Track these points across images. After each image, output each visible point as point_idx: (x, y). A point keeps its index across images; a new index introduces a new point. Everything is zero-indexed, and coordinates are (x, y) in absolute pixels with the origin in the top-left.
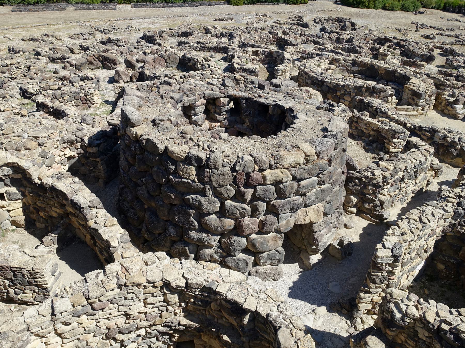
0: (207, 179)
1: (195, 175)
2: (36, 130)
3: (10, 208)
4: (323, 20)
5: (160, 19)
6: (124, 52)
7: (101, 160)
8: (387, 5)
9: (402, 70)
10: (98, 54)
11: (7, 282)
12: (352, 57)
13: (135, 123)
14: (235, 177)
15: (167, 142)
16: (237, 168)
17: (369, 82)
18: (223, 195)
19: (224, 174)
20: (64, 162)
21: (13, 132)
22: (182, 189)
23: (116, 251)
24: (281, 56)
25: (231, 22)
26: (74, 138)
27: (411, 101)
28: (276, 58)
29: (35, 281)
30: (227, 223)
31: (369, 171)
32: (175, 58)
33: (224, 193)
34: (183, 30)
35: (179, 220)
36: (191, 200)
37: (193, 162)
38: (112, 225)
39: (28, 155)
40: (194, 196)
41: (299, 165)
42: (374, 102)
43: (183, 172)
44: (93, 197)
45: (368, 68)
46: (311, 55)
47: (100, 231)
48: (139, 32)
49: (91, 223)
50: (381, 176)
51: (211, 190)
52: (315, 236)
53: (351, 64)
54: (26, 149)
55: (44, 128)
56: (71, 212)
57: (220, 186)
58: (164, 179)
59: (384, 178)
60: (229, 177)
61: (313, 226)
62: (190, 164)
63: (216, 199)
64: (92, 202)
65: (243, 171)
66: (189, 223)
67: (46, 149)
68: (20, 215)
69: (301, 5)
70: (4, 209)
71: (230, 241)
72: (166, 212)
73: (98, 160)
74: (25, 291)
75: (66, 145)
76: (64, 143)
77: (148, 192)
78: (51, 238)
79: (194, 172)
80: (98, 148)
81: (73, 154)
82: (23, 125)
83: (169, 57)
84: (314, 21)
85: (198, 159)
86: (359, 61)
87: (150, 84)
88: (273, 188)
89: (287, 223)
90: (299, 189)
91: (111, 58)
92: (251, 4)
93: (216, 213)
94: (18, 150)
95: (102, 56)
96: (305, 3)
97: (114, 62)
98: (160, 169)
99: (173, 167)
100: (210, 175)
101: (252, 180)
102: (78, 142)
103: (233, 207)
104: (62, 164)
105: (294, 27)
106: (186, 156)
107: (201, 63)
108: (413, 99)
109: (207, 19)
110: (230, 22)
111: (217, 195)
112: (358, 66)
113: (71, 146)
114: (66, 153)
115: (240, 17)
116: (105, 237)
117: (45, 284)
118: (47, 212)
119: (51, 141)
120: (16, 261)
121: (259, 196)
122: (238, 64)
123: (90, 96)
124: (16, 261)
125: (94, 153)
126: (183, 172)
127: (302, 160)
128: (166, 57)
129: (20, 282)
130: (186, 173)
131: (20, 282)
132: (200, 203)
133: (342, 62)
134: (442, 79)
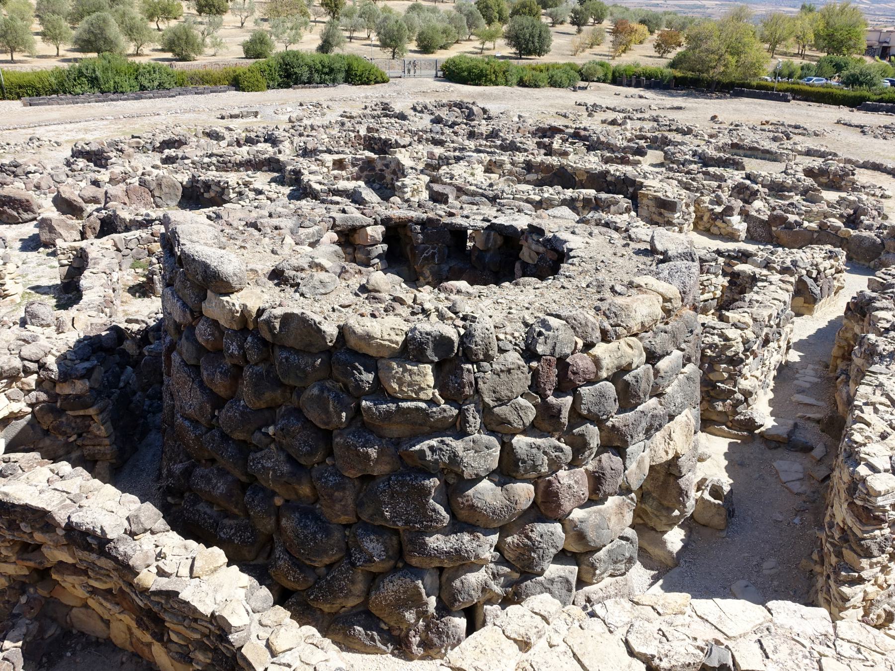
0: (468, 391)
4: (430, 107)
6: (44, 185)
7: (101, 411)
8: (526, 78)
9: (617, 170)
12: (520, 157)
13: (234, 282)
14: (535, 373)
15: (339, 317)
16: (540, 349)
17: (584, 191)
18: (509, 423)
19: (509, 371)
22: (395, 430)
23: (247, 638)
24: (393, 166)
25: (255, 119)
26: (17, 363)
27: (656, 218)
28: (382, 170)
30: (522, 494)
31: (713, 334)
32: (173, 186)
33: (513, 417)
34: (161, 138)
35: (396, 515)
36: (428, 453)
37: (430, 353)
38: (215, 570)
40: (434, 442)
42: (618, 221)
43: (400, 382)
44: (132, 502)
45: (555, 174)
46: (445, 161)
47: (184, 595)
49: (149, 579)
50: (740, 340)
51: (478, 417)
52: (683, 487)
53: (523, 168)
56: (61, 562)
57: (501, 402)
58: (344, 414)
59: (746, 342)
60: (521, 376)
61: (680, 464)
62: (420, 358)
63: (492, 438)
64: (137, 517)
66: (425, 515)
69: (377, 85)
71: (529, 538)
72: (350, 501)
73: (91, 411)
77: (291, 460)
79: (431, 380)
80: (89, 379)
81: (15, 407)
83: (160, 185)
84: (414, 109)
85: (443, 342)
86: (537, 162)
87: (144, 235)
88: (610, 388)
90: (659, 380)
91: (18, 197)
92: (282, 88)
93: (491, 475)
96: (384, 82)
97: (24, 206)
98: (329, 390)
99: (370, 377)
100: (476, 379)
101: (574, 373)
102: (27, 372)
103: (534, 451)
105: (385, 120)
106: (405, 342)
107: (237, 190)
108: (661, 214)
109: (204, 117)
110: (252, 119)
111: (494, 427)
112: (536, 172)
115: (270, 111)
116: (206, 608)
121: (589, 410)
122: (320, 183)
125: (78, 397)
126: (400, 385)
128: (153, 186)
130: (410, 385)
132: (454, 458)
133: (508, 166)
134: (684, 180)
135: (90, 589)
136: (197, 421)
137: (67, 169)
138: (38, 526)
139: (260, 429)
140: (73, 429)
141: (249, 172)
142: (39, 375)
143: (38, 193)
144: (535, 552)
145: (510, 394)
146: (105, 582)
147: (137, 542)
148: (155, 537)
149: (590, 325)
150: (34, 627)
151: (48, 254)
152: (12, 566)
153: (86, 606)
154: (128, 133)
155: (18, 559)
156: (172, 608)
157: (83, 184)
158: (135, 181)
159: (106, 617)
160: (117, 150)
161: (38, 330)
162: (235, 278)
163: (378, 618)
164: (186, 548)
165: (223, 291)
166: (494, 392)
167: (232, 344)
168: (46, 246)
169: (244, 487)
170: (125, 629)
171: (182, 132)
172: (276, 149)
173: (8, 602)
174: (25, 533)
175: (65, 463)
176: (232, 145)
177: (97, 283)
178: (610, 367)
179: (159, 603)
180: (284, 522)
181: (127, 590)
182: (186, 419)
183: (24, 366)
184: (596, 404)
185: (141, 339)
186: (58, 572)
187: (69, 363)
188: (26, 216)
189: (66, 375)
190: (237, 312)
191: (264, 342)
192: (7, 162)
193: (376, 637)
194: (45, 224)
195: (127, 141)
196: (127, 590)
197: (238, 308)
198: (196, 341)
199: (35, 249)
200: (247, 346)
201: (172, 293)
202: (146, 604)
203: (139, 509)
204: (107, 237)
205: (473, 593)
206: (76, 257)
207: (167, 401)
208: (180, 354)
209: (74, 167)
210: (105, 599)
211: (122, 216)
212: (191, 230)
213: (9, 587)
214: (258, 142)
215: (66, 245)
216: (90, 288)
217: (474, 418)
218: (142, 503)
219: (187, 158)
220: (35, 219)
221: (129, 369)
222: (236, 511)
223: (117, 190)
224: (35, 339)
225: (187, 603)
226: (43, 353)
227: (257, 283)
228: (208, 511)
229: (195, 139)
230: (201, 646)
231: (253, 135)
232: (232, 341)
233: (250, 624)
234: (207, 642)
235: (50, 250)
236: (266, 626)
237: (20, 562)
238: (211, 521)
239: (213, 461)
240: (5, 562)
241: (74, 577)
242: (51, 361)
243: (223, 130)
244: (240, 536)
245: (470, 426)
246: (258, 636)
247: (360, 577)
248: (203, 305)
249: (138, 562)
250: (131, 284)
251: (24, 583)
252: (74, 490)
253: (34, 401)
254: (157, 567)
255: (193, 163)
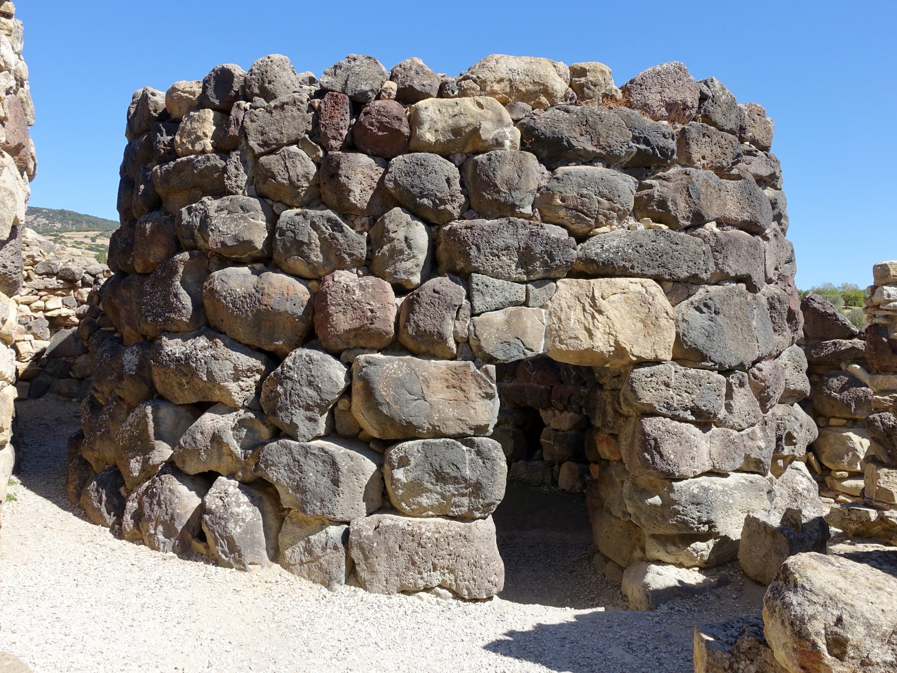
1: (210, 134)
41: (546, 91)
57: (272, 148)
58: (142, 187)
60: (296, 113)
63: (255, 203)
65: (344, 92)
75: (53, 282)
89: (508, 322)
102: (85, 284)
121: (396, 182)
127: (560, 86)
144: (281, 385)
145: (278, 136)
149: (414, 67)
166: (262, 135)
178: (439, 126)
184: (407, 174)
205: (199, 437)
217: (236, 168)
245: (229, 178)
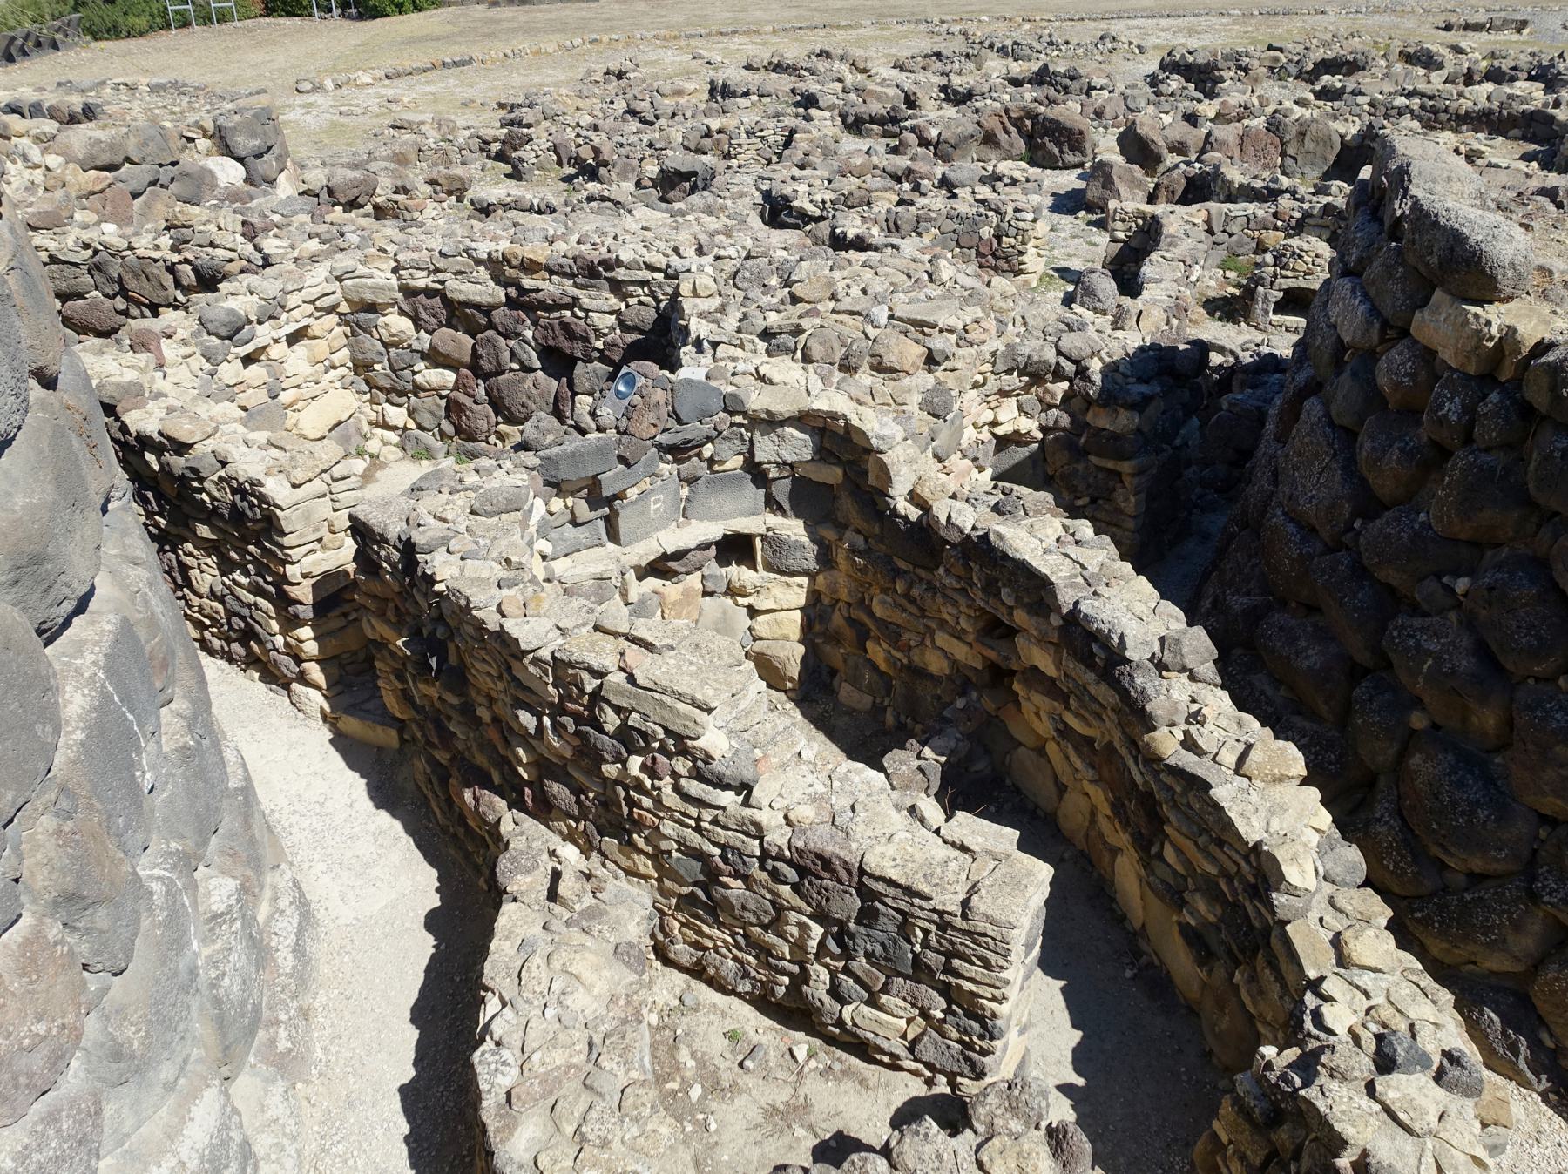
2: (920, 300)
3: (761, 603)
5: (1214, 20)
6: (1109, 112)
7: (1139, 472)
10: (1023, 109)
11: (817, 931)
13: (1505, 280)
20: (986, 454)
21: (833, 297)
23: (1303, 913)
25: (1516, 37)
26: (1050, 355)
29: (949, 970)
32: (1326, 141)
34: (1319, 55)
38: (1280, 779)
39: (884, 394)
44: (1172, 619)
48: (1142, 58)
49: (1167, 743)
54: (879, 368)
55: (943, 298)
56: (1035, 668)
64: (1177, 642)
67: (951, 381)
68: (787, 639)
70: (740, 600)
73: (1126, 467)
74: (884, 999)
75: (1014, 381)
76: (1009, 372)
77: (1483, 651)
78: (917, 763)
80: (1140, 413)
82: (868, 274)
83: (1302, 135)
87: (1260, 213)
91: (1069, 124)
94: (848, 368)
95: (1034, 116)
97: (1072, 139)
102: (1059, 375)
104: (975, 460)
109: (1410, 23)
110: (1509, 36)
113: (1026, 389)
114: (1001, 418)
116: (1251, 829)
117: (994, 999)
118: (907, 649)
119: (972, 350)
120: (891, 850)
123: (1012, 241)
124: (891, 850)
125: (1115, 437)
129: (879, 950)
131: (879, 950)
135: (1061, 726)
136: (1313, 529)
137: (1150, 90)
138: (1026, 600)
139: (1438, 576)
140: (1089, 486)
141: (1480, 135)
142: (1072, 385)
143: (1096, 123)
146: (1089, 725)
147: (1165, 682)
148: (1195, 686)
150: (965, 746)
151: (1089, 223)
152: (965, 648)
153: (1041, 751)
154: (1260, 42)
155: (977, 640)
156: (1189, 806)
157: (1167, 119)
158: (1259, 123)
159: (1064, 780)
160: (1239, 67)
161: (1088, 315)
162: (1510, 273)
163: (1539, 1017)
164: (1240, 724)
165: (1474, 294)
167: (1451, 400)
168: (1090, 210)
169: (1356, 673)
170: (1086, 812)
171: (1360, 47)
172: (1551, 98)
173: (939, 698)
174: (1004, 604)
175: (1087, 522)
176: (1453, 82)
177: (1168, 276)
179: (1170, 788)
180: (1416, 760)
181: (1123, 751)
182: (1292, 520)
183: (1058, 364)
185: (1218, 382)
186: (1027, 683)
187: (1120, 379)
188: (1071, 158)
189: (1110, 397)
190: (1491, 338)
191: (1527, 411)
192: (1062, 70)
193: (1523, 1049)
194: (1102, 173)
195: (1257, 54)
196: (1123, 751)
197: (1494, 330)
198: (1372, 382)
199: (1072, 211)
200: (1482, 409)
201: (1353, 291)
202: (1146, 782)
203: (1184, 632)
204: (1197, 206)
206: (1140, 229)
207: (1262, 481)
208: (1326, 404)
209: (1162, 87)
210: (1076, 749)
211: (1229, 177)
212: (1437, 173)
213: (949, 678)
214: (1513, 79)
215: (1130, 206)
216: (1156, 281)
218: (1190, 624)
219: (1361, 93)
220: (1081, 165)
221: (1195, 421)
222: (1323, 709)
223: (1228, 133)
224: (1082, 327)
225: (1217, 808)
226: (1089, 351)
227: (1545, 295)
228: (1269, 691)
229: (1383, 63)
230: (1210, 890)
231: (1505, 66)
232: (1454, 393)
233: (1314, 894)
234: (1224, 888)
235: (1094, 217)
236: (1341, 911)
237: (978, 646)
238: (1270, 710)
239: (1312, 609)
240: (959, 638)
241: (1046, 699)
242: (1095, 366)
243: (1444, 51)
244: (1316, 754)
246: (1321, 920)
247: (1535, 926)
248: (1418, 314)
249: (1160, 712)
250: (1212, 294)
251: (967, 681)
252: (1093, 568)
253: (1051, 424)
254: (1186, 733)
255: (1371, 104)
